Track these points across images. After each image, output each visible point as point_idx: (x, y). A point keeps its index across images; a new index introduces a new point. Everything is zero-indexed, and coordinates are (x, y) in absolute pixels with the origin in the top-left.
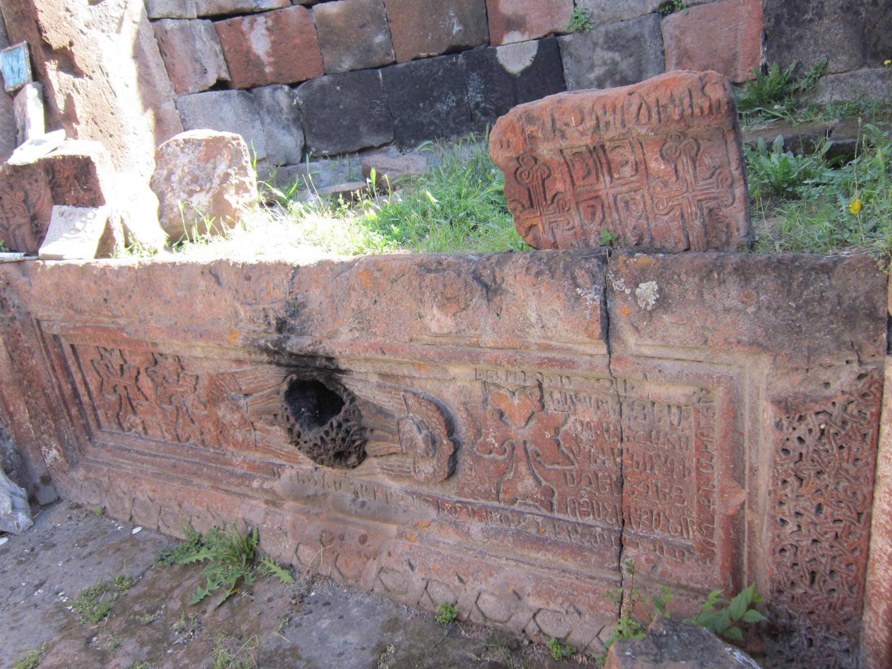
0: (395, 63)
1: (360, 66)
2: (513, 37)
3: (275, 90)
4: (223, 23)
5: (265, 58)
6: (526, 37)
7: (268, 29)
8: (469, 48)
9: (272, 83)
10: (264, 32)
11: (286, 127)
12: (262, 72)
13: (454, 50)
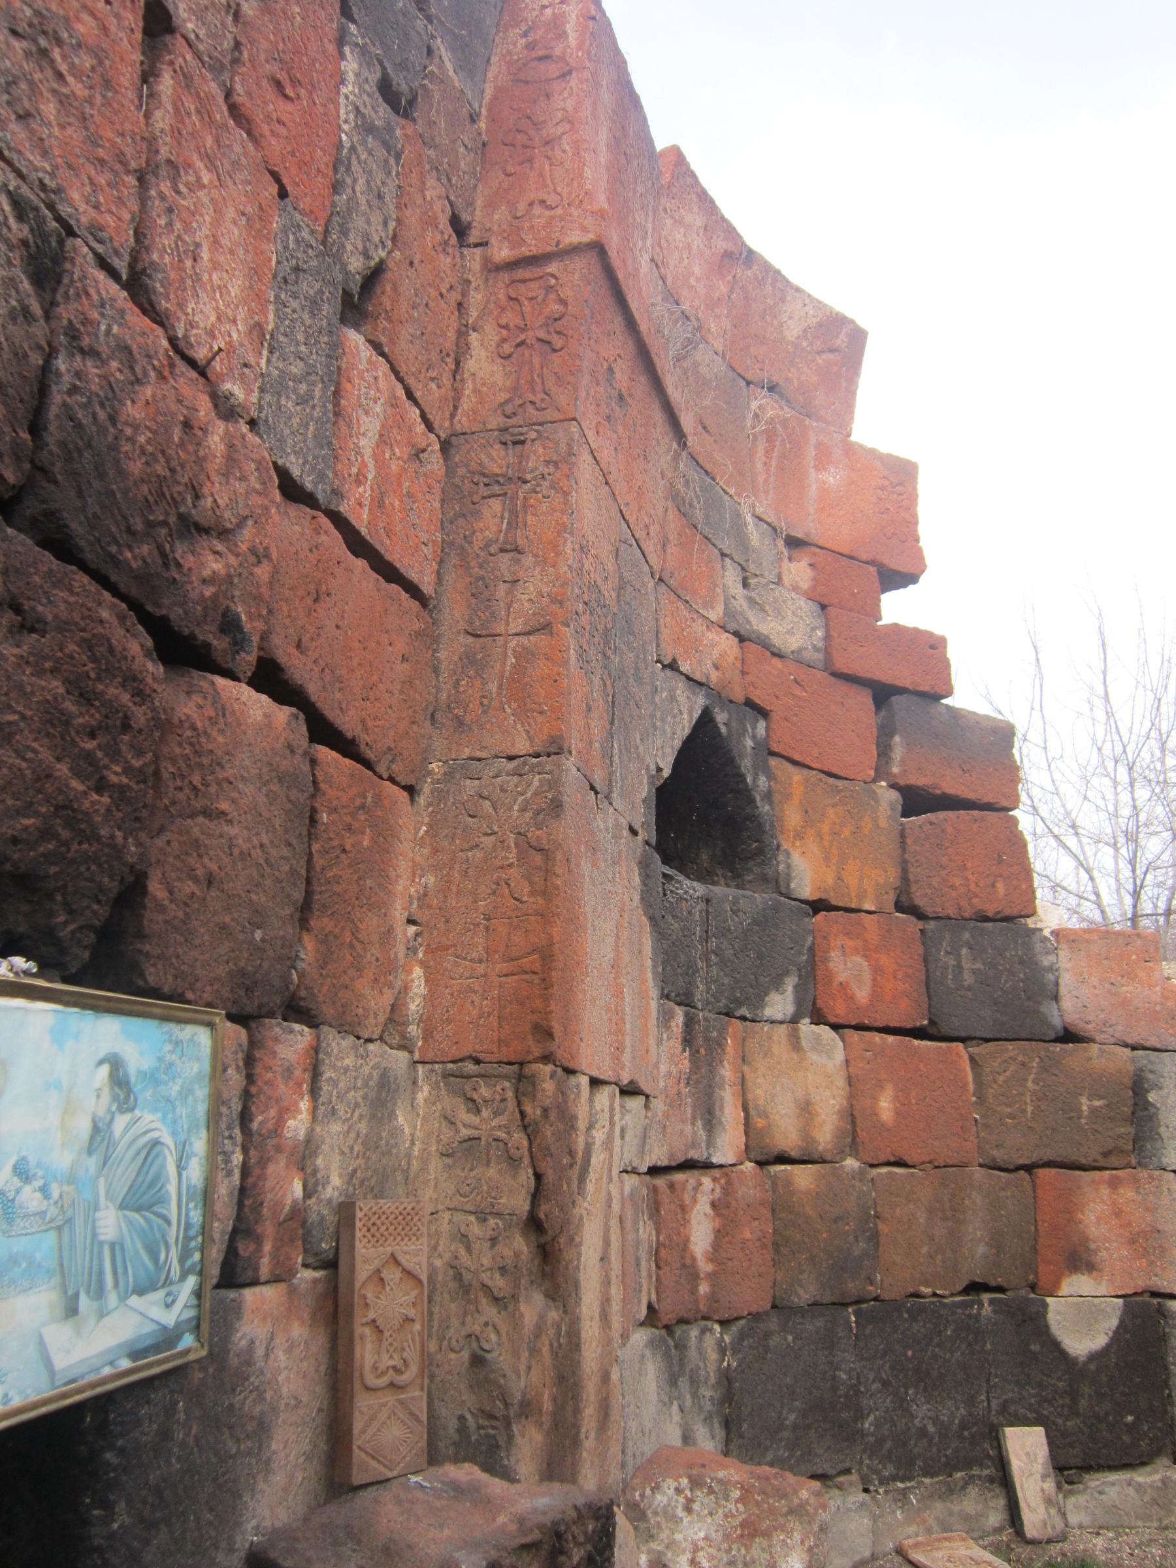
1: (828, 1298)
2: (1077, 1284)
3: (703, 1332)
4: (660, 1182)
5: (705, 1267)
6: (1103, 1290)
7: (713, 1205)
8: (1000, 1289)
9: (705, 1318)
10: (709, 1210)
11: (708, 1419)
12: (694, 1291)
13: (975, 1287)
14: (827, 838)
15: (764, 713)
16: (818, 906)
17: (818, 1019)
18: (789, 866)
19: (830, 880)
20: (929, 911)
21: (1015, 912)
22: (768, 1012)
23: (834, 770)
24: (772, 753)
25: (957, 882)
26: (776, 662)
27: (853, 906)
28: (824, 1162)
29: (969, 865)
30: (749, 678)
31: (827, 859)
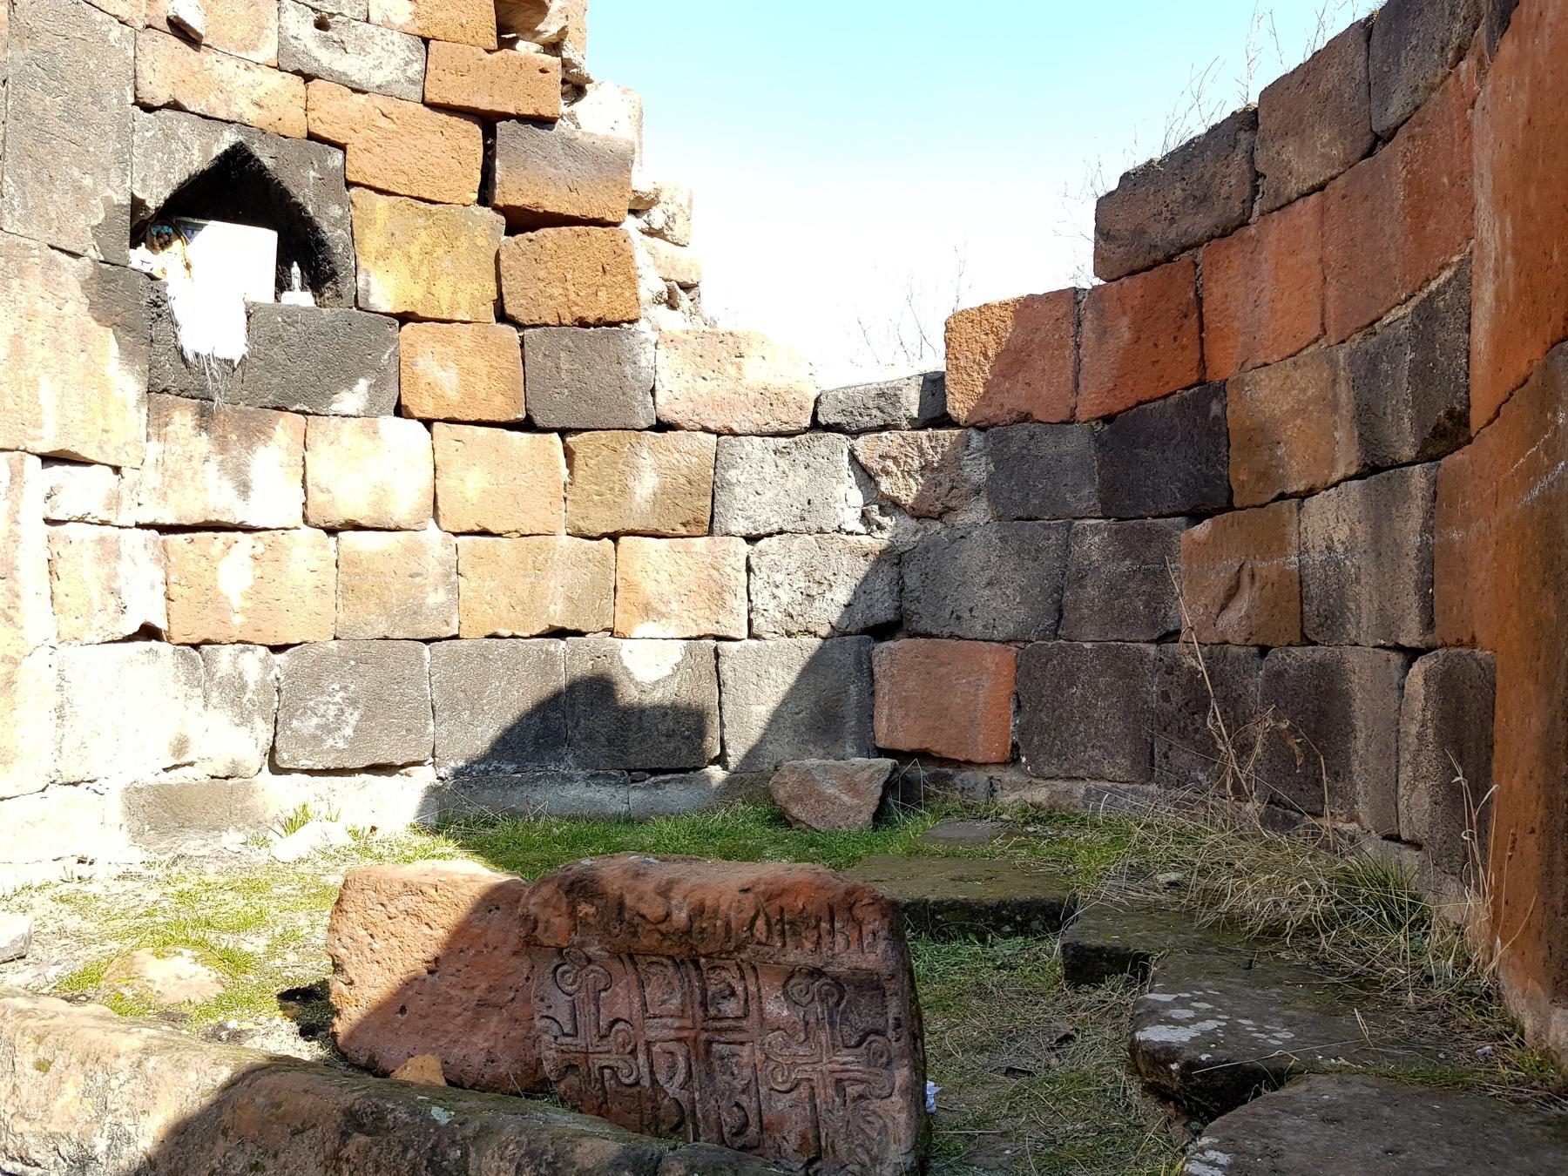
0: (456, 637)
5: (237, 602)
13: (559, 633)
14: (416, 257)
15: (342, 147)
16: (404, 318)
17: (400, 411)
18: (368, 283)
19: (418, 296)
20: (524, 320)
21: (617, 318)
22: (335, 407)
23: (426, 196)
24: (349, 184)
25: (556, 292)
26: (361, 98)
27: (444, 317)
28: (398, 529)
29: (569, 277)
30: (311, 115)
31: (415, 274)
